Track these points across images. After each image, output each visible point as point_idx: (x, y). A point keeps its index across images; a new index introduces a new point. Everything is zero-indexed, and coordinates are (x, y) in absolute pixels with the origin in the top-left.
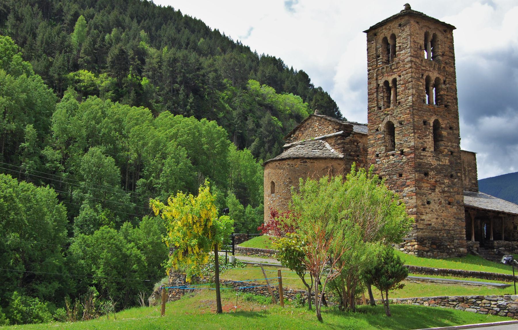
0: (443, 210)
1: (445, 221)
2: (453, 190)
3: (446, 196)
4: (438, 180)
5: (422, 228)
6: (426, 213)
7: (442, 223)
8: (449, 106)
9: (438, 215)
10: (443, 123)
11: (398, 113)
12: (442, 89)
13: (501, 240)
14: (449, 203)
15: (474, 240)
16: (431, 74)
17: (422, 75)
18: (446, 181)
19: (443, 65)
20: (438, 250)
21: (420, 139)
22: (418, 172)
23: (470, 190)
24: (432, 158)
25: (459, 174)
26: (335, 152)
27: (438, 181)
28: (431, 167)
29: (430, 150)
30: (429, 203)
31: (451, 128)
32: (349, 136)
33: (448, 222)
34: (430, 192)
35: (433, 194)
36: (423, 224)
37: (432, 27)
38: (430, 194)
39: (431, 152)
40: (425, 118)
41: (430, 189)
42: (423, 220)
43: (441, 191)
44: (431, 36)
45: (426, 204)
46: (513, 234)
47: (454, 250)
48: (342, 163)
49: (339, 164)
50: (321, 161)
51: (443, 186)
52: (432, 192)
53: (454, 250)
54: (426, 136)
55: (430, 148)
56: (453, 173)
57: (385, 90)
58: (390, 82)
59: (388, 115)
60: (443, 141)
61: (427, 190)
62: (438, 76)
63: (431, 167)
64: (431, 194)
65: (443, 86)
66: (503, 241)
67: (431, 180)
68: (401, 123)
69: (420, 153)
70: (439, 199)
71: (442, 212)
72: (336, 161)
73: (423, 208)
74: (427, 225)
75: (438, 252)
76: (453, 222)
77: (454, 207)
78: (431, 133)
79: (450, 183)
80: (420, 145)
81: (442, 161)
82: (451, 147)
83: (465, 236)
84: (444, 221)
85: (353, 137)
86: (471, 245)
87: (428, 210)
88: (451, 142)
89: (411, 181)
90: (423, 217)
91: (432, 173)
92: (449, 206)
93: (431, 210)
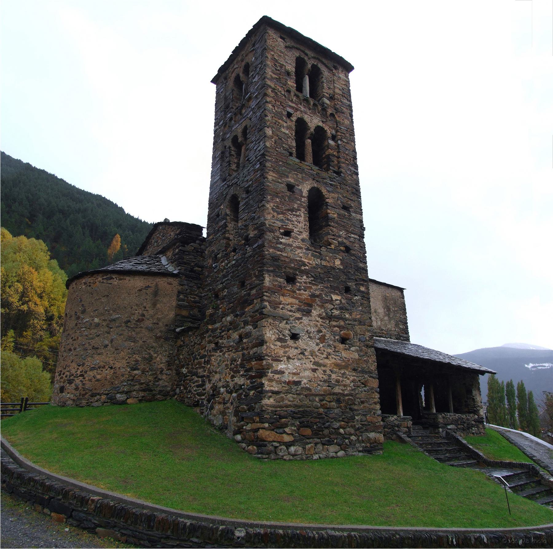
0: (329, 354)
1: (334, 376)
2: (351, 314)
3: (335, 326)
4: (317, 293)
5: (276, 389)
6: (289, 358)
7: (325, 381)
8: (341, 172)
9: (315, 363)
10: (331, 198)
11: (244, 176)
12: (328, 146)
13: (449, 412)
14: (343, 340)
15: (402, 414)
16: (307, 118)
17: (289, 115)
18: (334, 297)
19: (330, 111)
20: (318, 440)
21: (278, 214)
22: (272, 274)
23: (397, 339)
24: (304, 251)
25: (362, 289)
26: (171, 267)
27: (317, 296)
28: (303, 268)
29: (300, 237)
30: (295, 337)
31: (346, 208)
32: (195, 242)
33: (341, 379)
34: (298, 315)
35: (305, 320)
36: (279, 382)
37: (310, 54)
38: (299, 319)
39: (303, 240)
40: (292, 181)
41: (298, 310)
42: (282, 372)
43: (324, 314)
44: (309, 66)
45: (288, 338)
46: (466, 402)
47: (353, 438)
48: (175, 282)
49: (170, 284)
50: (137, 278)
51: (330, 306)
52: (303, 315)
53: (353, 438)
54: (292, 210)
55: (301, 232)
56: (352, 285)
57: (233, 153)
58: (239, 134)
59: (232, 185)
60: (330, 226)
61: (291, 311)
62: (321, 124)
63: (303, 268)
64: (301, 318)
65: (331, 142)
66: (452, 414)
67: (302, 292)
68: (248, 192)
69: (278, 238)
70: (320, 331)
71: (327, 358)
72: (165, 279)
73: (281, 346)
74: (289, 383)
75: (316, 444)
76: (352, 378)
77: (353, 349)
78: (304, 208)
79: (343, 301)
80: (279, 224)
81: (325, 260)
82: (345, 238)
83: (378, 407)
84: (330, 376)
85: (200, 245)
86: (397, 423)
87: (292, 352)
88: (347, 231)
89: (256, 291)
90: (281, 366)
91: (303, 279)
92: (342, 346)
93: (299, 351)
